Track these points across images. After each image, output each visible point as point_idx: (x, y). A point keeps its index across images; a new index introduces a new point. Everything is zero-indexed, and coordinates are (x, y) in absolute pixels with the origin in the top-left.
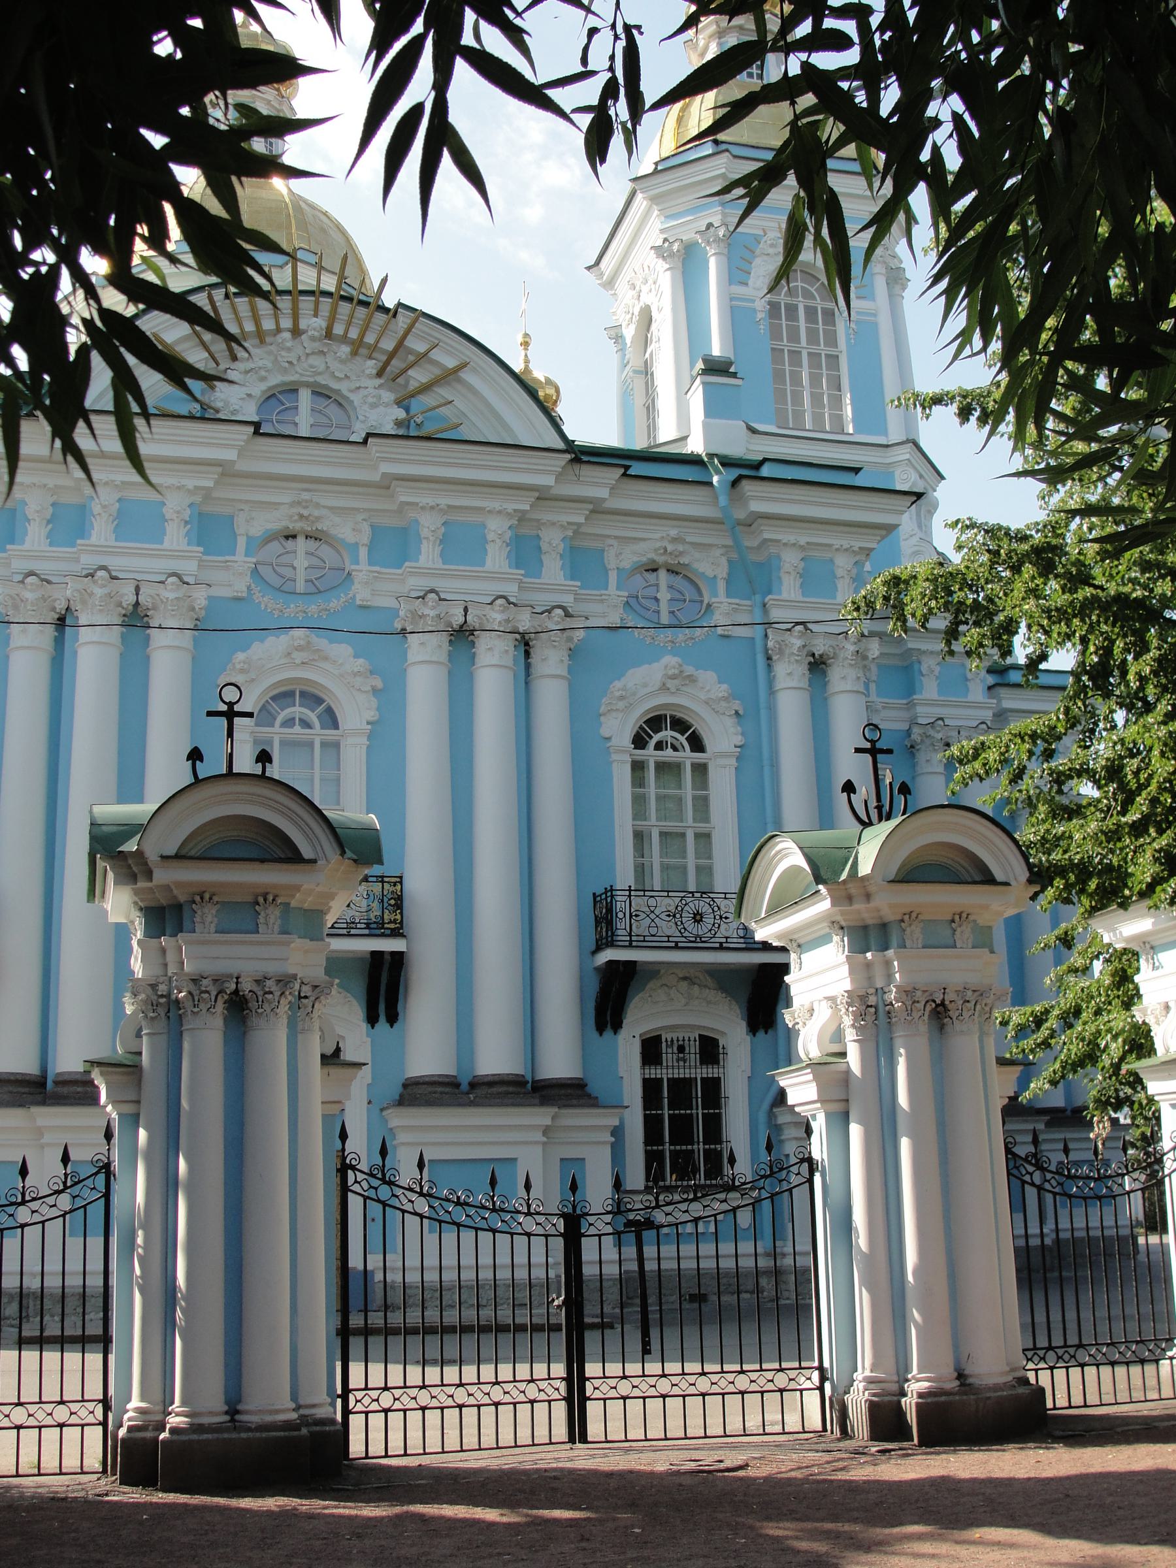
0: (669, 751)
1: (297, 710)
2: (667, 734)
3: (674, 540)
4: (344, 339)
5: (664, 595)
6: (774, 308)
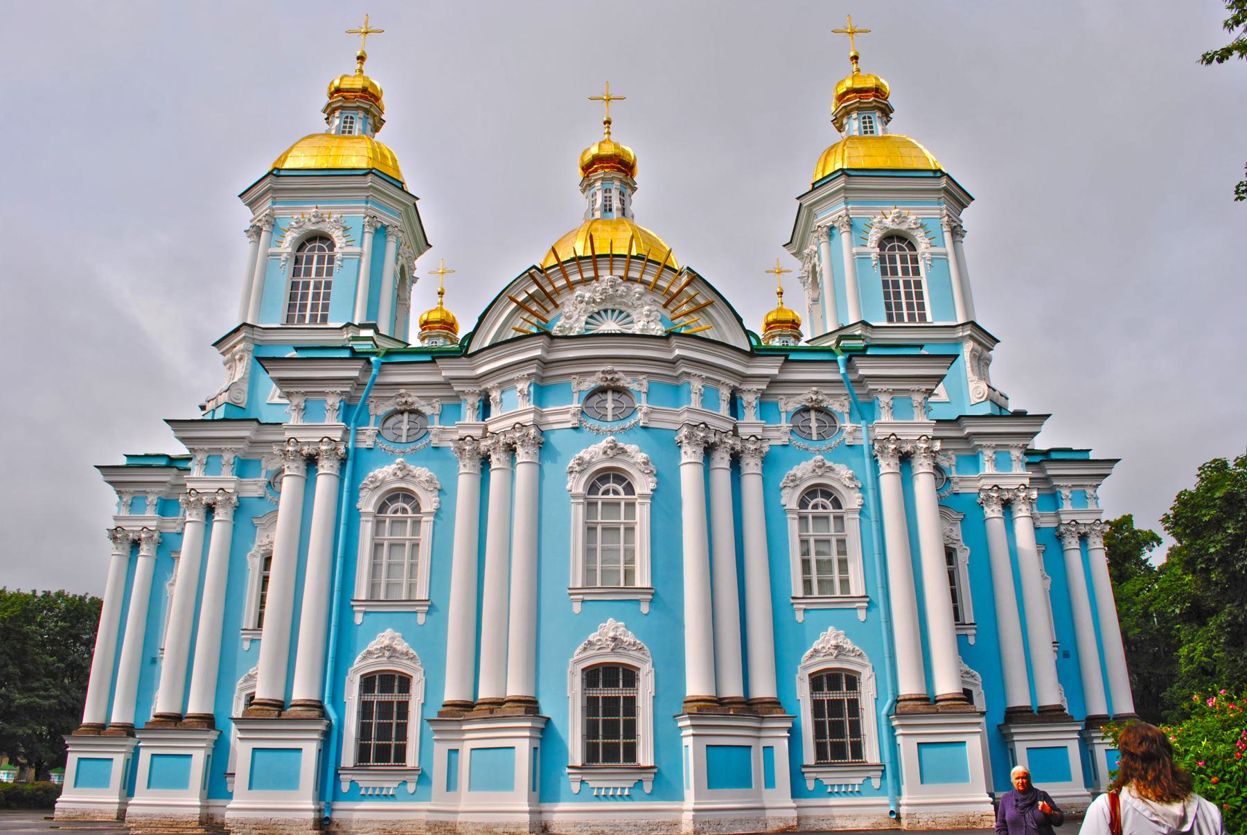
0: (820, 510)
2: (819, 500)
3: (817, 393)
5: (814, 424)
6: (882, 259)
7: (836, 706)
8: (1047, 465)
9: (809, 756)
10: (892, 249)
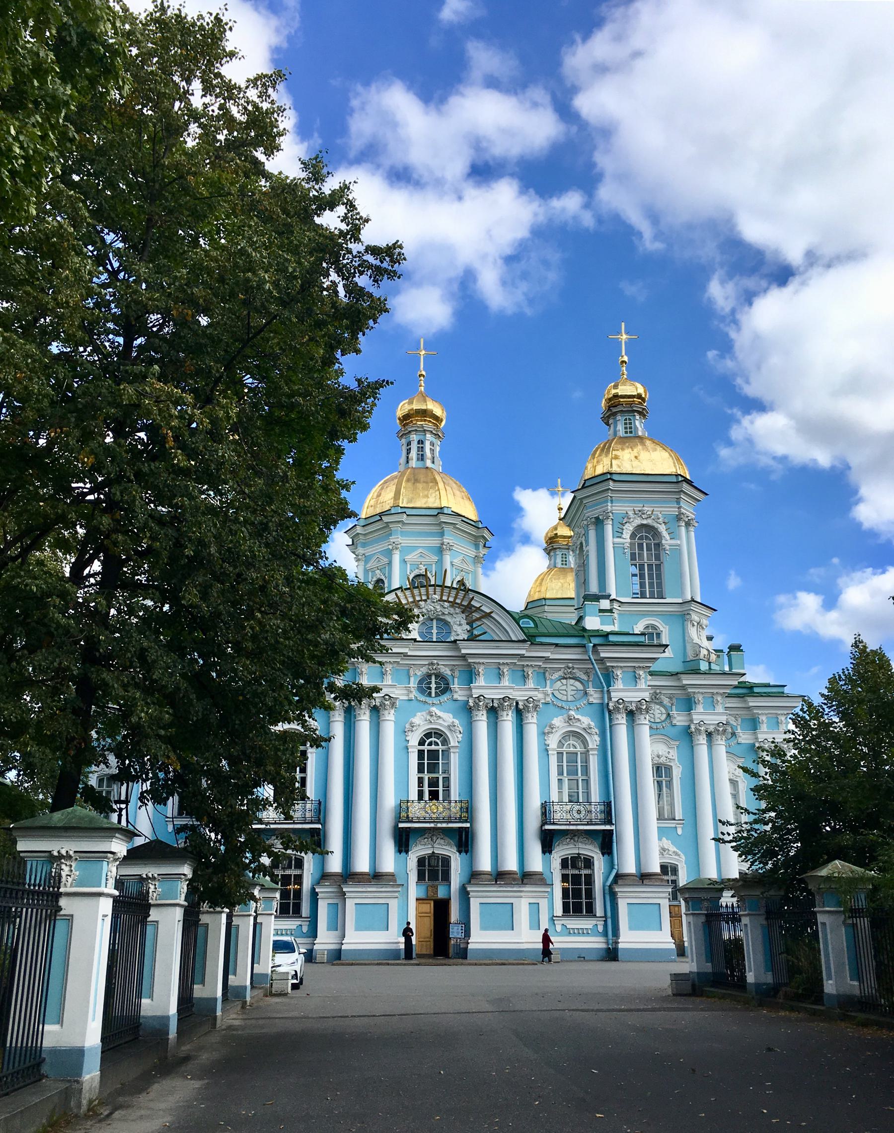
1: (433, 739)
4: (447, 601)
7: (576, 879)
8: (749, 699)
9: (559, 910)
10: (641, 538)
